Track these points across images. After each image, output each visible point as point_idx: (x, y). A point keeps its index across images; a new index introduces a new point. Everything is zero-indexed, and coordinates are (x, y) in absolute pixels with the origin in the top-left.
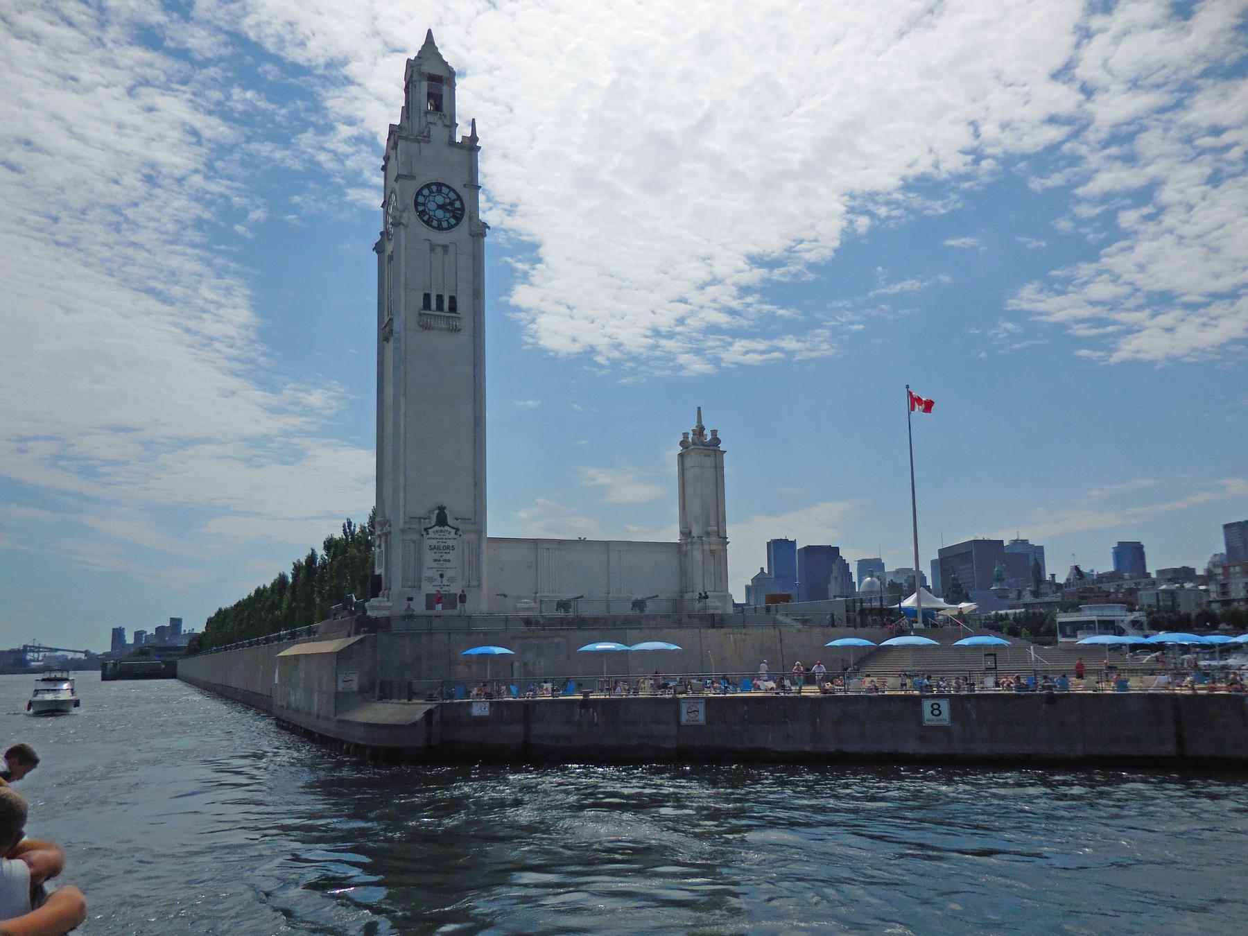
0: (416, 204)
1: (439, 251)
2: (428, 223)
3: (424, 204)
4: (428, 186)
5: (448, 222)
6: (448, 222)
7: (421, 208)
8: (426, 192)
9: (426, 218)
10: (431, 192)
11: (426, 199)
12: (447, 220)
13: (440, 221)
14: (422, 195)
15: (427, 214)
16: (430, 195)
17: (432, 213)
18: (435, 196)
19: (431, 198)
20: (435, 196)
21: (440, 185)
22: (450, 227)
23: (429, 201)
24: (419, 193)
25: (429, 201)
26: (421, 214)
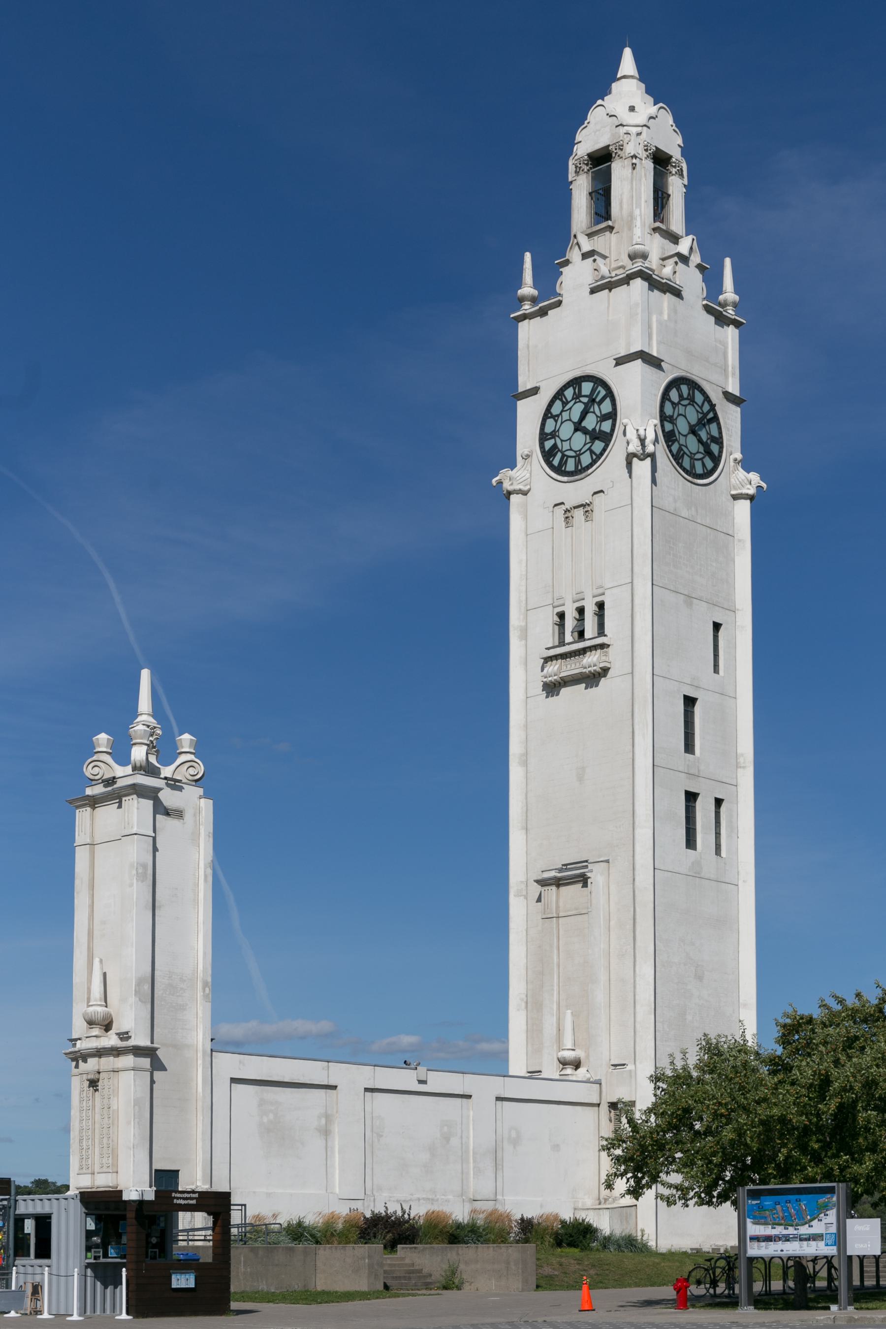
0: (543, 437)
1: (579, 514)
2: (559, 470)
3: (554, 434)
4: (559, 395)
5: (592, 452)
6: (592, 452)
7: (548, 444)
8: (557, 408)
9: (556, 462)
10: (565, 404)
11: (556, 421)
12: (589, 449)
13: (578, 455)
14: (553, 417)
15: (559, 450)
16: (562, 411)
17: (566, 446)
18: (570, 409)
19: (565, 415)
20: (570, 409)
21: (576, 382)
22: (596, 458)
23: (562, 423)
24: (548, 414)
25: (562, 423)
26: (548, 455)
